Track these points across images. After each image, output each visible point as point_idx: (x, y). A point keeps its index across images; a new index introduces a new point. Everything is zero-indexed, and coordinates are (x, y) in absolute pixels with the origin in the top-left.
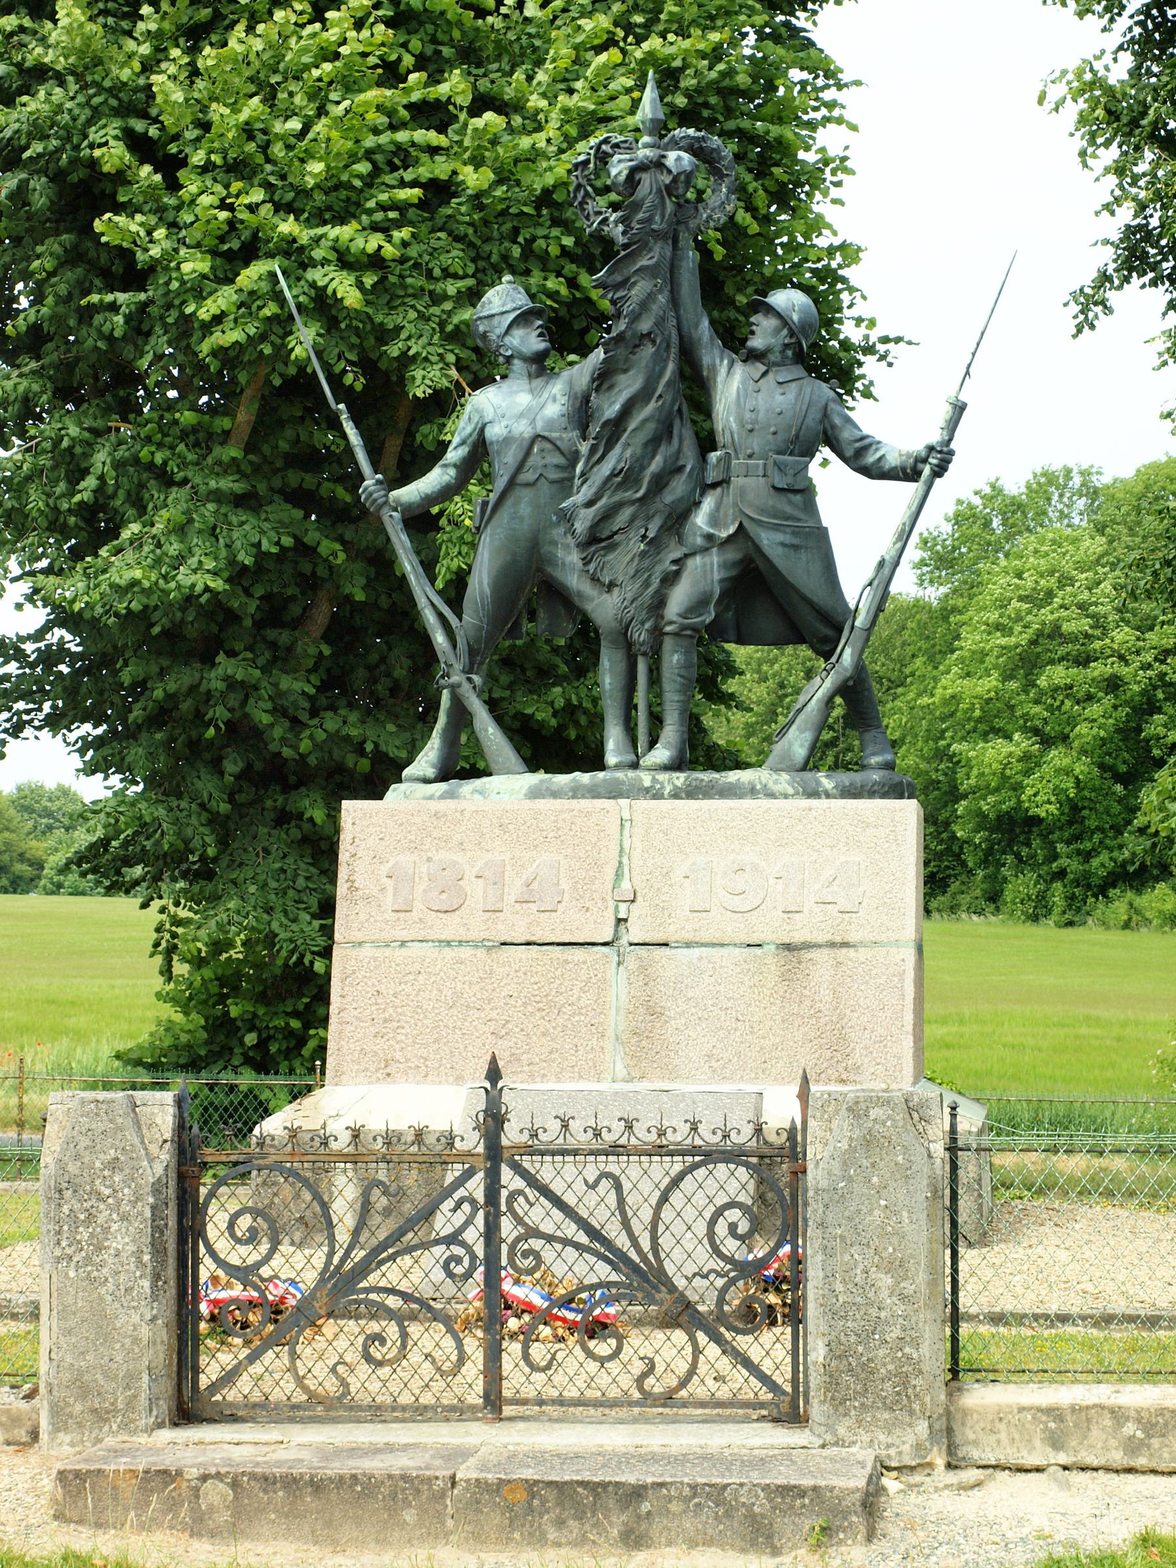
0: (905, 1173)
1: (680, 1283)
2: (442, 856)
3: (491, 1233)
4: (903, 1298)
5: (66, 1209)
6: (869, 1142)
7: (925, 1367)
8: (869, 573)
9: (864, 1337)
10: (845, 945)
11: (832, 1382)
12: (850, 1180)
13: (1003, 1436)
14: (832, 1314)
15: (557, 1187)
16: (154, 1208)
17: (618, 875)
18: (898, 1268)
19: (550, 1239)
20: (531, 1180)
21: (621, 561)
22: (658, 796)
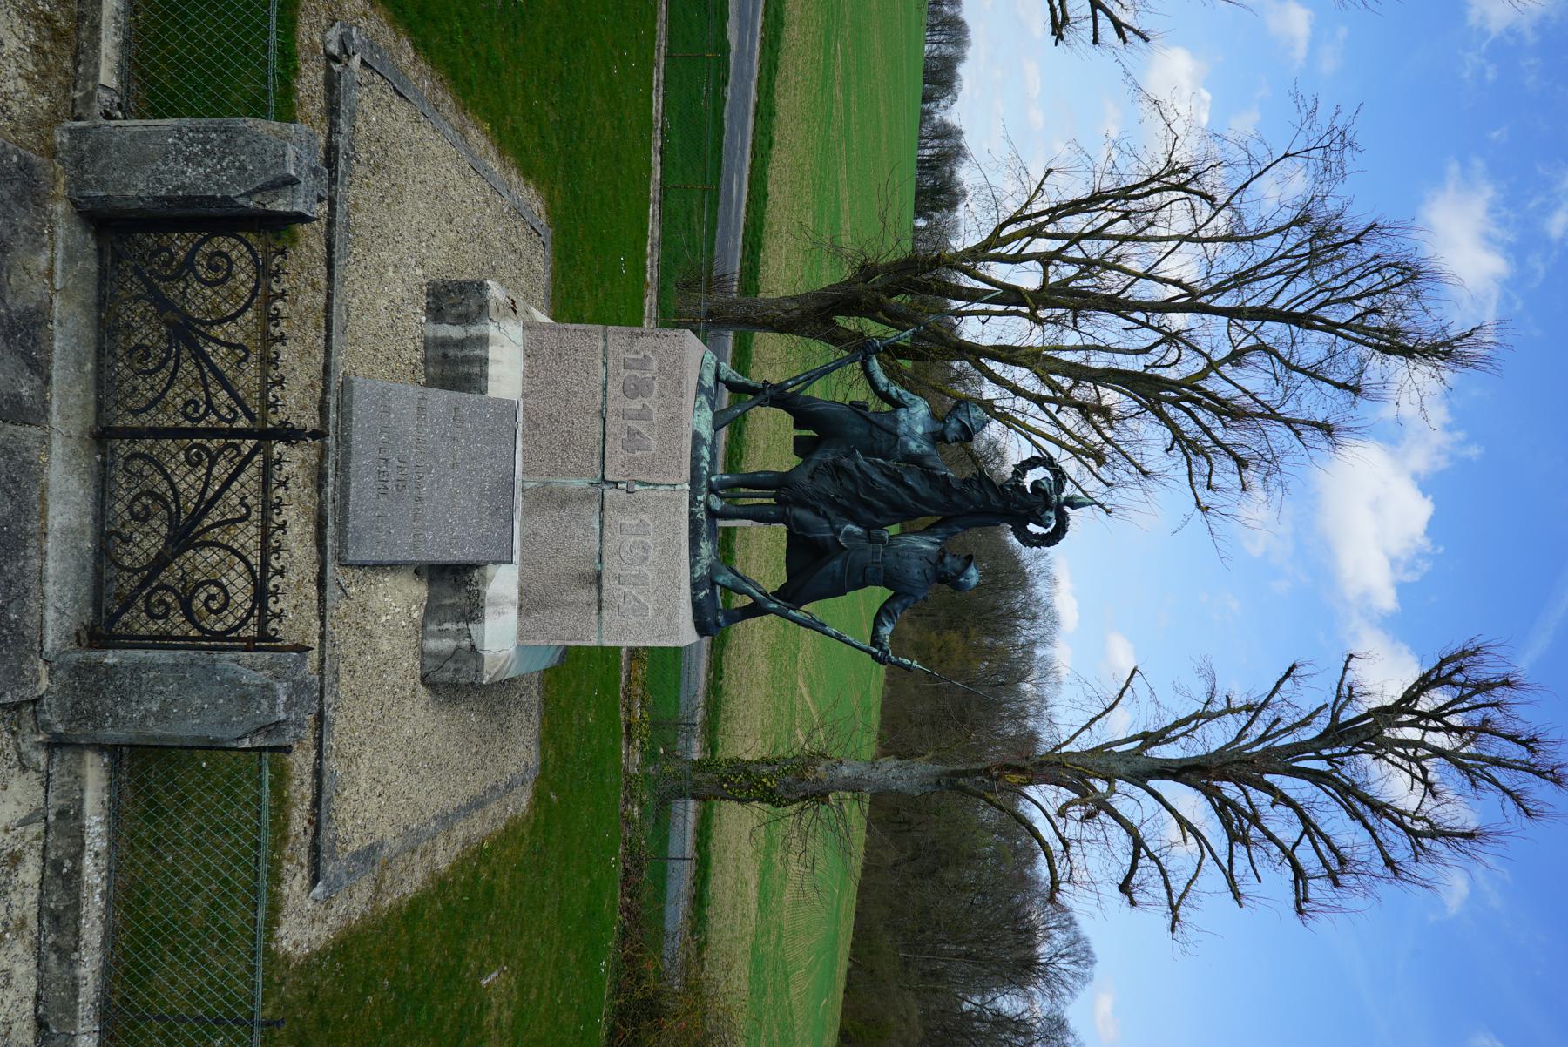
0: (225, 722)
1: (179, 560)
2: (656, 385)
3: (212, 433)
4: (144, 718)
5: (214, 135)
6: (247, 698)
7: (99, 732)
8: (818, 617)
9: (119, 691)
10: (600, 609)
11: (93, 667)
12: (221, 684)
13: (66, 779)
14: (136, 669)
15: (243, 477)
16: (214, 197)
17: (643, 484)
18: (163, 715)
19: (209, 474)
20: (248, 459)
21: (827, 485)
22: (691, 504)
